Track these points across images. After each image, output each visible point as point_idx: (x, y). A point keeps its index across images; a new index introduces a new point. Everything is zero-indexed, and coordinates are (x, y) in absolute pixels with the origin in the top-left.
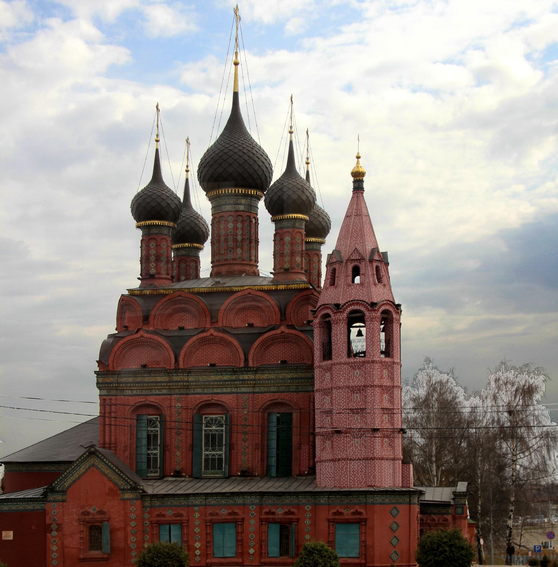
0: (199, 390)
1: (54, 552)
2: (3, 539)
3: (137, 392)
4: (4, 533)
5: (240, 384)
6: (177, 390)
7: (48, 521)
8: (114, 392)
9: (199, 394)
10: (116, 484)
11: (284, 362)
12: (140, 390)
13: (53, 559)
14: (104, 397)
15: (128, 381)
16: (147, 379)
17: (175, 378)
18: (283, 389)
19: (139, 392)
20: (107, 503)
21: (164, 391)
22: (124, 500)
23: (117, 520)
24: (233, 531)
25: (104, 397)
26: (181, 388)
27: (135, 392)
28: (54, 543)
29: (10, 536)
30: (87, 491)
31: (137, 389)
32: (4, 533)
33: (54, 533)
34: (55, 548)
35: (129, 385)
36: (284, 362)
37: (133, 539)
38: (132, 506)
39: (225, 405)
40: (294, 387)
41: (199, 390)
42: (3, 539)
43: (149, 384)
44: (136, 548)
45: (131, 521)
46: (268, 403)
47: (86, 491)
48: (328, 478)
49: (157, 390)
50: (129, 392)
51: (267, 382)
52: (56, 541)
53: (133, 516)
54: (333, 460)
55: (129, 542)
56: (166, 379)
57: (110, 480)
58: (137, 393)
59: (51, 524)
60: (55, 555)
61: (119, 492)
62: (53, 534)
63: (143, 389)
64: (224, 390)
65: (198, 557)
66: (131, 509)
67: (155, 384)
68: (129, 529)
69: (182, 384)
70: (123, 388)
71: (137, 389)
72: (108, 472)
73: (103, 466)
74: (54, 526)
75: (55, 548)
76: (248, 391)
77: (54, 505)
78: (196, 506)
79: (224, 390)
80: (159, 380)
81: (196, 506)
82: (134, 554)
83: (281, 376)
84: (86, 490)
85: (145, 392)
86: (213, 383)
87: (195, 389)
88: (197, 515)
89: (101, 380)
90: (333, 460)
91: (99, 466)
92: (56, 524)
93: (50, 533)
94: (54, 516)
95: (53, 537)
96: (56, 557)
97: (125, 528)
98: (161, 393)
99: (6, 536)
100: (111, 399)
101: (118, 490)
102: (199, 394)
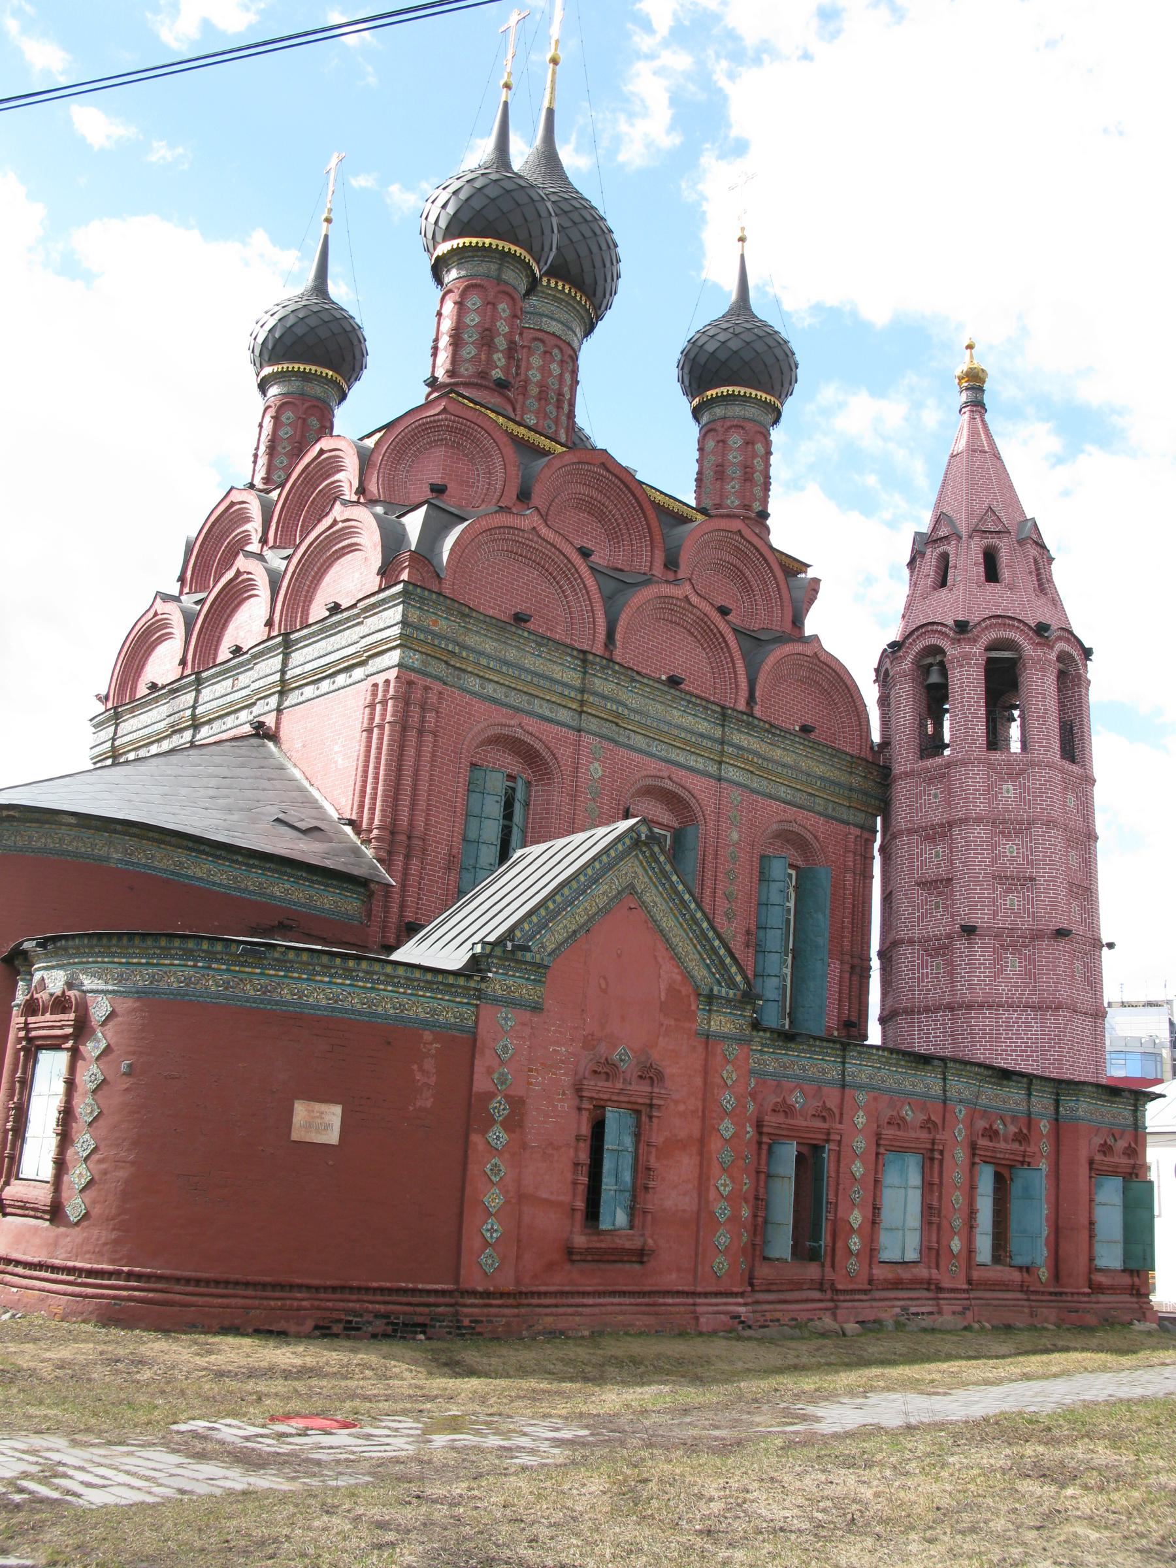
0: (639, 741)
1: (490, 1214)
2: (295, 1136)
3: (495, 691)
4: (301, 1111)
5: (731, 756)
6: (595, 720)
7: (481, 1084)
8: (439, 669)
9: (640, 751)
10: (687, 975)
11: (806, 729)
12: (504, 690)
13: (487, 1244)
14: (413, 676)
15: (480, 648)
16: (529, 662)
17: (599, 684)
18: (800, 798)
19: (500, 693)
20: (661, 1038)
21: (563, 715)
22: (707, 1038)
23: (682, 1108)
24: (915, 1179)
25: (413, 676)
26: (606, 720)
27: (490, 689)
28: (493, 1178)
29: (328, 1127)
30: (607, 985)
31: (497, 683)
32: (301, 1111)
33: (497, 1136)
34: (494, 1199)
35: (484, 661)
36: (806, 729)
37: (725, 1185)
38: (728, 1062)
39: (694, 805)
40: (822, 802)
41: (639, 741)
42: (295, 1136)
43: (535, 680)
44: (729, 1219)
45: (722, 1120)
46: (775, 827)
47: (603, 986)
48: (1016, 1051)
49: (545, 705)
50: (474, 684)
51: (780, 770)
52: (502, 1168)
53: (728, 1100)
54: (1039, 1007)
55: (712, 1194)
56: (572, 677)
57: (676, 958)
58: (495, 695)
59: (491, 1096)
60: (492, 1229)
61: (693, 1007)
62: (491, 1136)
63: (515, 689)
64: (692, 761)
65: (853, 1260)
66: (725, 1075)
67: (547, 684)
68: (715, 1145)
69: (614, 708)
70: (464, 667)
71: (497, 683)
72: (669, 923)
73: (658, 900)
74: (499, 1107)
75: (494, 1199)
76: (741, 780)
77: (506, 1019)
78: (860, 1087)
79: (692, 761)
80: (558, 677)
81: (860, 1087)
82: (723, 1240)
83: (804, 765)
84: (605, 978)
85: (515, 699)
86: (676, 732)
87: (632, 734)
88: (860, 1120)
89: (414, 617)
90: (1039, 1007)
91: (647, 898)
92: (506, 1097)
93: (484, 1131)
94: (502, 1063)
95: (492, 1150)
96: (497, 1239)
97: (702, 1143)
98: (553, 716)
99: (309, 1126)
100: (427, 688)
101: (692, 998)
102: (640, 751)
